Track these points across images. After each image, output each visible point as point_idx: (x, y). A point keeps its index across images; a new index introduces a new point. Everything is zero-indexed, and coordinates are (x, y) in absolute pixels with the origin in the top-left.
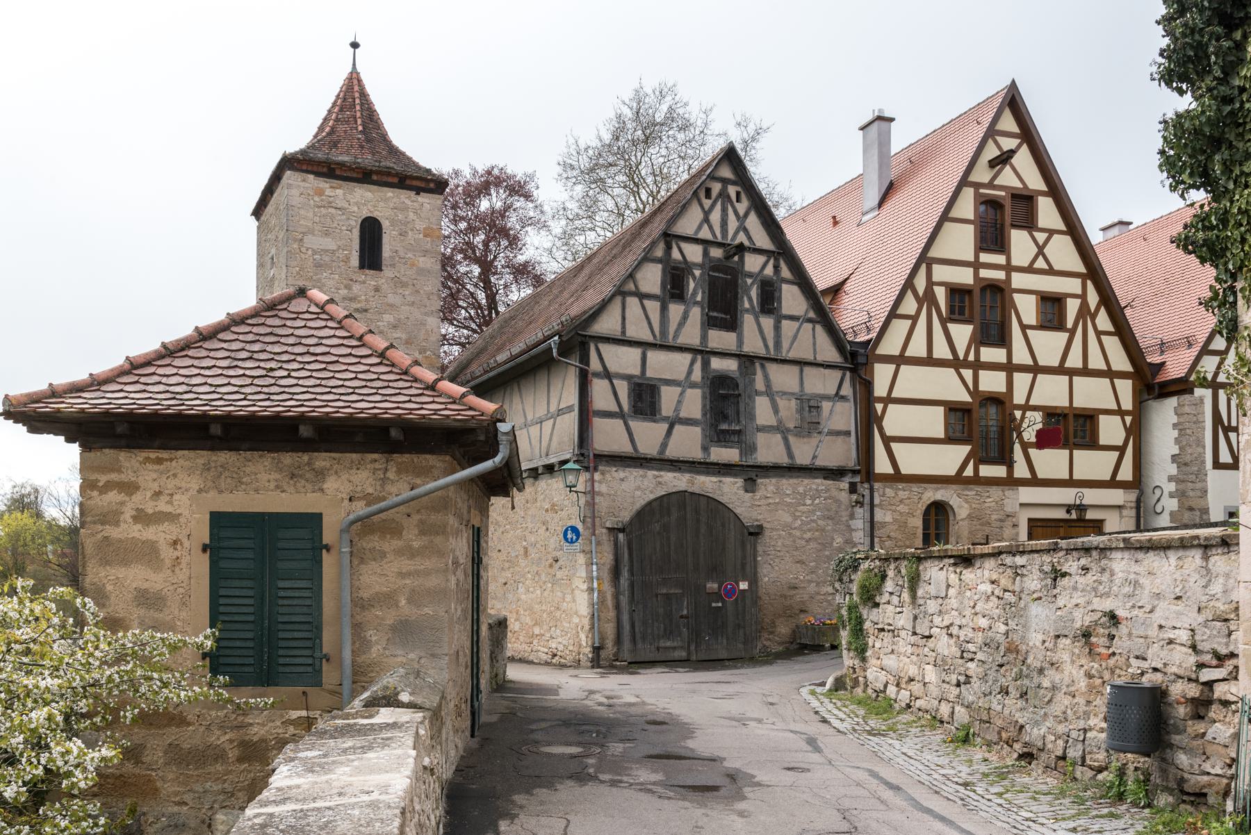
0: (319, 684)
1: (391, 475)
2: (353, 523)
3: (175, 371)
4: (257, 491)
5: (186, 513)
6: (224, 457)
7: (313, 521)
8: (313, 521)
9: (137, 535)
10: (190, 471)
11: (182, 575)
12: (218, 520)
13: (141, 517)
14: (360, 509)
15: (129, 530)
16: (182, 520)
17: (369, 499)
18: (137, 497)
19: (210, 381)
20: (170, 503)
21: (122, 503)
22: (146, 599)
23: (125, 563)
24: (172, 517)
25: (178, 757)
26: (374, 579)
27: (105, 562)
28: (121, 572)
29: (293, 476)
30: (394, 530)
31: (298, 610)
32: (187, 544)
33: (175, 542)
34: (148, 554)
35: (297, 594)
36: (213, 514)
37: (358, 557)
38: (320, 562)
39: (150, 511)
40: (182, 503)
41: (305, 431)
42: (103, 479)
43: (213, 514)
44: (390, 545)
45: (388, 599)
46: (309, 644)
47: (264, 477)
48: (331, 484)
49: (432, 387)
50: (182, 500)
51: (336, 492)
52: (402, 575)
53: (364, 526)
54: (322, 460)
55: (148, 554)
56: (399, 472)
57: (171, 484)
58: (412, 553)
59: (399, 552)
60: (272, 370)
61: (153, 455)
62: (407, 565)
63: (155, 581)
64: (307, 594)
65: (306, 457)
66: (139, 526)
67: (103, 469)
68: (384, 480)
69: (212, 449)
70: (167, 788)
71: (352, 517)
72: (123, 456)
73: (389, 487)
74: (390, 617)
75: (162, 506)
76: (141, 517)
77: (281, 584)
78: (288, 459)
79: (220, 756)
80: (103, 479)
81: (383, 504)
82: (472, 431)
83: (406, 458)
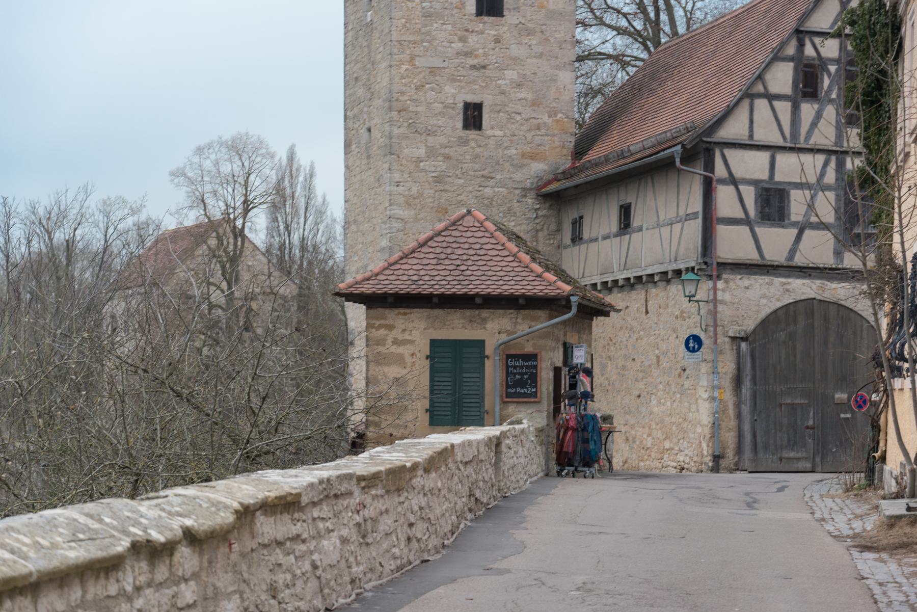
1: (519, 320)
2: (501, 345)
3: (410, 267)
4: (453, 329)
5: (418, 340)
6: (437, 312)
7: (481, 344)
8: (481, 344)
9: (394, 351)
12: (434, 343)
13: (396, 342)
16: (416, 343)
17: (509, 333)
18: (394, 332)
19: (429, 272)
20: (410, 334)
21: (387, 335)
28: (386, 369)
29: (471, 321)
31: (473, 388)
32: (418, 355)
33: (413, 354)
34: (399, 360)
35: (472, 380)
36: (431, 340)
38: (484, 364)
39: (400, 339)
43: (431, 340)
46: (478, 405)
48: (489, 325)
49: (540, 276)
54: (485, 313)
55: (399, 360)
56: (523, 319)
57: (411, 326)
60: (458, 266)
61: (402, 311)
64: (477, 380)
65: (477, 312)
66: (395, 346)
67: (377, 318)
68: (516, 323)
69: (432, 308)
71: (500, 342)
72: (387, 311)
73: (518, 327)
75: (407, 336)
77: (465, 375)
78: (468, 313)
80: (378, 323)
81: (515, 336)
82: (559, 299)
83: (526, 312)
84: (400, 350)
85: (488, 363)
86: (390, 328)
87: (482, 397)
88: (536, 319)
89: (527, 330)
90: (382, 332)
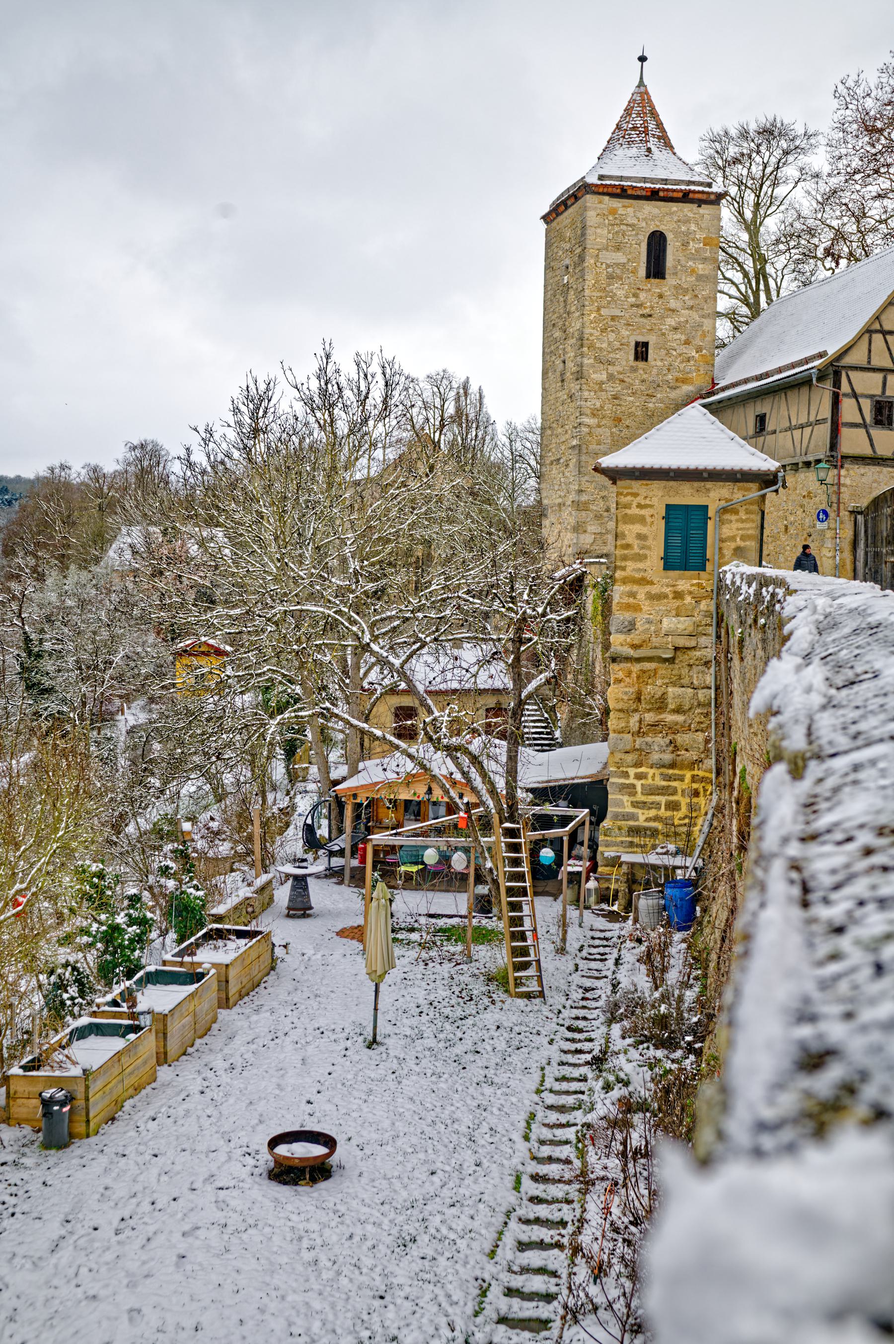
0: (704, 570)
6: (672, 483)
10: (659, 489)
11: (654, 528)
13: (639, 506)
14: (723, 504)
15: (634, 511)
17: (727, 500)
18: (638, 499)
22: (641, 537)
23: (633, 523)
24: (651, 506)
25: (651, 597)
26: (726, 531)
27: (625, 523)
28: (631, 527)
30: (736, 512)
34: (642, 520)
36: (668, 506)
37: (722, 522)
40: (655, 501)
41: (705, 475)
42: (625, 491)
44: (734, 518)
45: (733, 538)
47: (686, 491)
48: (712, 494)
50: (655, 499)
51: (714, 497)
52: (738, 529)
53: (724, 510)
54: (709, 485)
57: (651, 494)
58: (743, 521)
59: (737, 521)
61: (645, 482)
62: (741, 525)
63: (644, 530)
67: (626, 488)
70: (645, 608)
72: (633, 483)
73: (735, 496)
74: (733, 545)
75: (648, 502)
76: (639, 506)
79: (666, 596)
80: (625, 491)
83: (741, 484)
84: (643, 512)
85: (710, 524)
86: (636, 495)
87: (704, 548)
88: (749, 490)
89: (741, 499)
90: (629, 498)
